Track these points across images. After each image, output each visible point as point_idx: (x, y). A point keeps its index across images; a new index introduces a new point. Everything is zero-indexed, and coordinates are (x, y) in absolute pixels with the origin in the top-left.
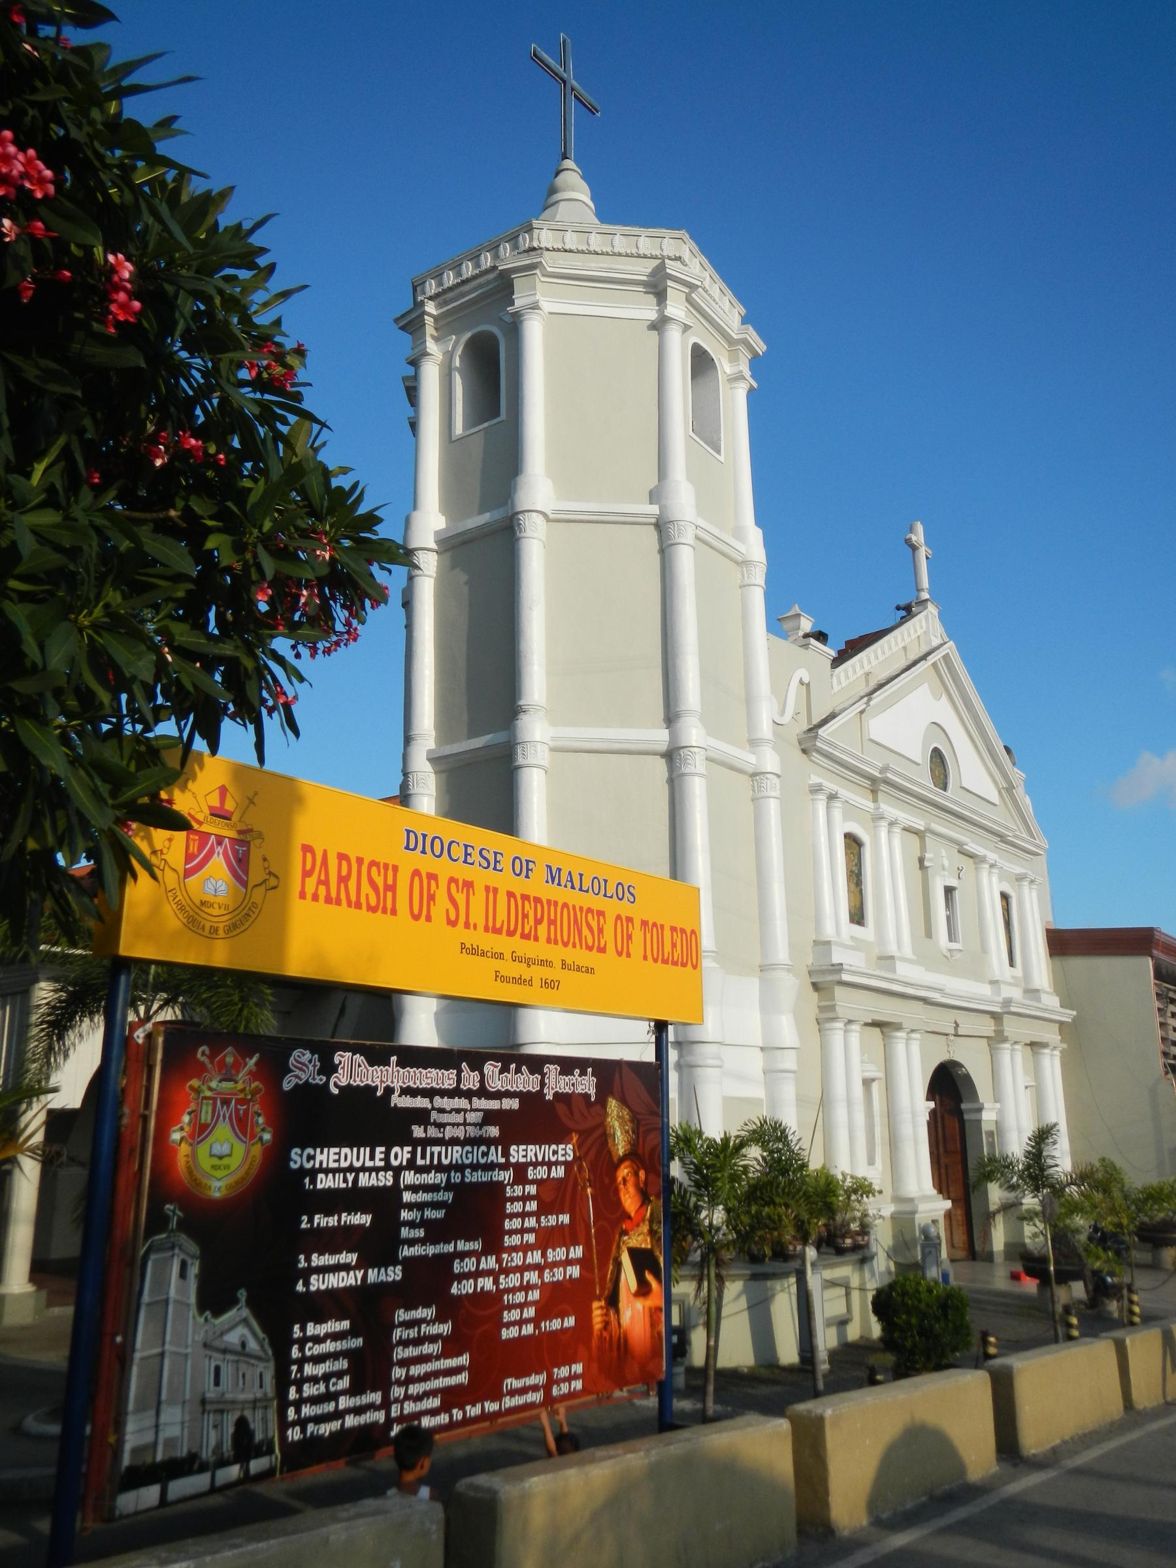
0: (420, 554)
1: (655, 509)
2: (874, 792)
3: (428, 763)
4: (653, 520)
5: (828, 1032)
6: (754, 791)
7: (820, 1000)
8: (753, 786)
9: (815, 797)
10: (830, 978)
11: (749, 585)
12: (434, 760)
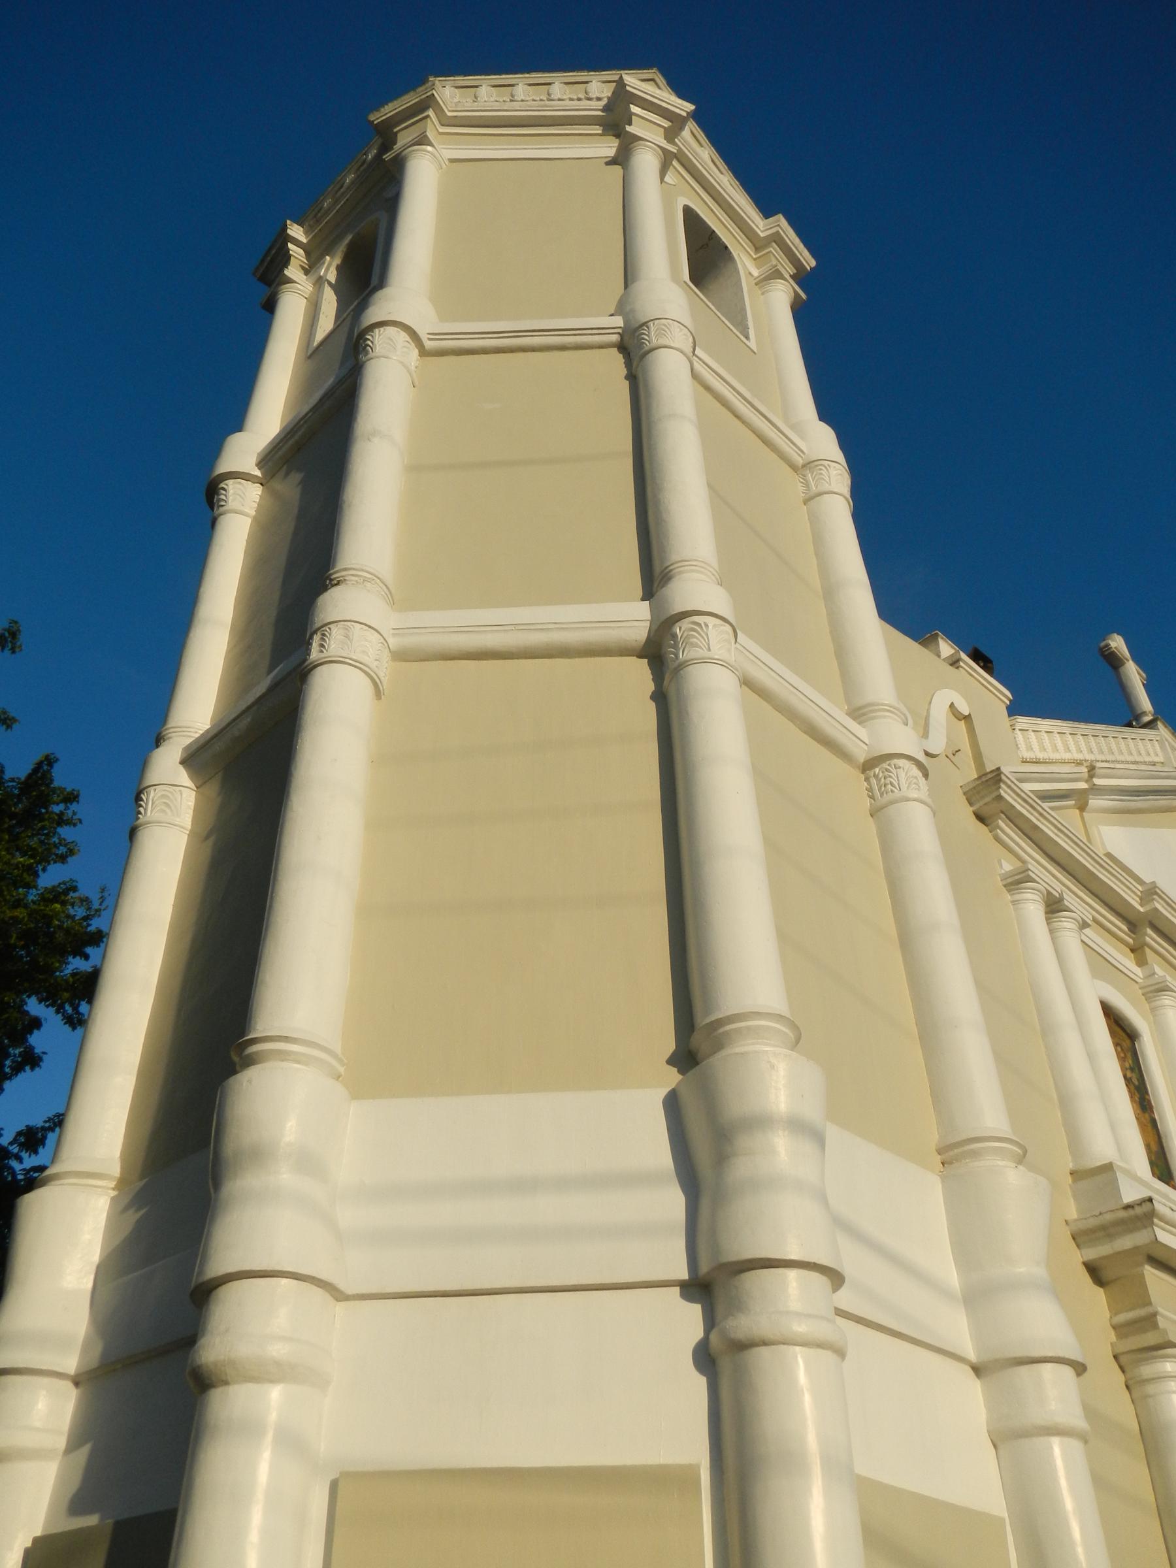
0: (231, 486)
1: (619, 321)
2: (1137, 950)
3: (181, 766)
4: (615, 338)
5: (1150, 1389)
6: (872, 797)
7: (1114, 1310)
8: (870, 790)
9: (1017, 897)
10: (1126, 1242)
11: (820, 494)
12: (193, 759)
